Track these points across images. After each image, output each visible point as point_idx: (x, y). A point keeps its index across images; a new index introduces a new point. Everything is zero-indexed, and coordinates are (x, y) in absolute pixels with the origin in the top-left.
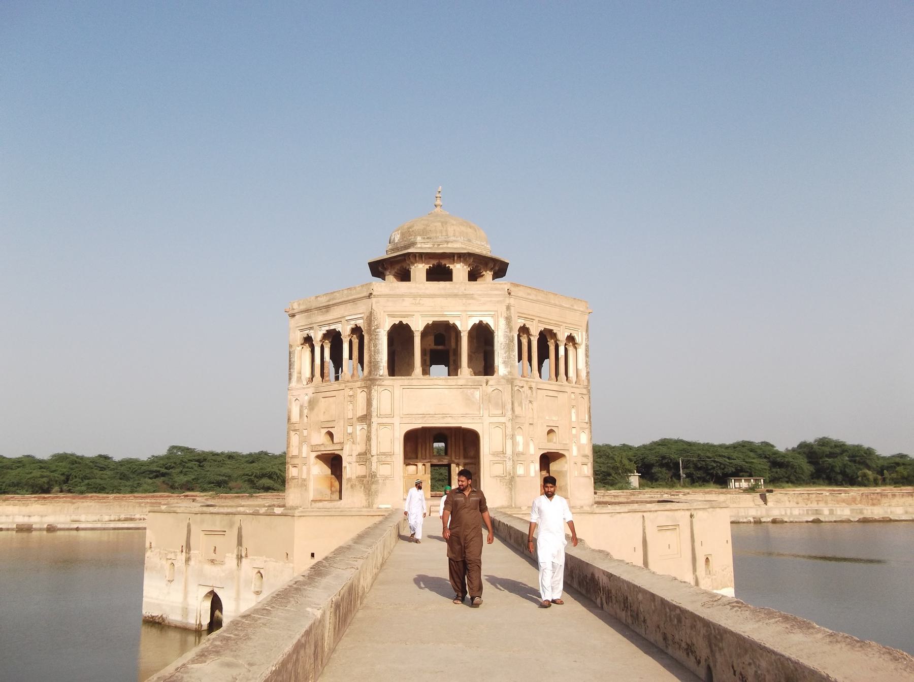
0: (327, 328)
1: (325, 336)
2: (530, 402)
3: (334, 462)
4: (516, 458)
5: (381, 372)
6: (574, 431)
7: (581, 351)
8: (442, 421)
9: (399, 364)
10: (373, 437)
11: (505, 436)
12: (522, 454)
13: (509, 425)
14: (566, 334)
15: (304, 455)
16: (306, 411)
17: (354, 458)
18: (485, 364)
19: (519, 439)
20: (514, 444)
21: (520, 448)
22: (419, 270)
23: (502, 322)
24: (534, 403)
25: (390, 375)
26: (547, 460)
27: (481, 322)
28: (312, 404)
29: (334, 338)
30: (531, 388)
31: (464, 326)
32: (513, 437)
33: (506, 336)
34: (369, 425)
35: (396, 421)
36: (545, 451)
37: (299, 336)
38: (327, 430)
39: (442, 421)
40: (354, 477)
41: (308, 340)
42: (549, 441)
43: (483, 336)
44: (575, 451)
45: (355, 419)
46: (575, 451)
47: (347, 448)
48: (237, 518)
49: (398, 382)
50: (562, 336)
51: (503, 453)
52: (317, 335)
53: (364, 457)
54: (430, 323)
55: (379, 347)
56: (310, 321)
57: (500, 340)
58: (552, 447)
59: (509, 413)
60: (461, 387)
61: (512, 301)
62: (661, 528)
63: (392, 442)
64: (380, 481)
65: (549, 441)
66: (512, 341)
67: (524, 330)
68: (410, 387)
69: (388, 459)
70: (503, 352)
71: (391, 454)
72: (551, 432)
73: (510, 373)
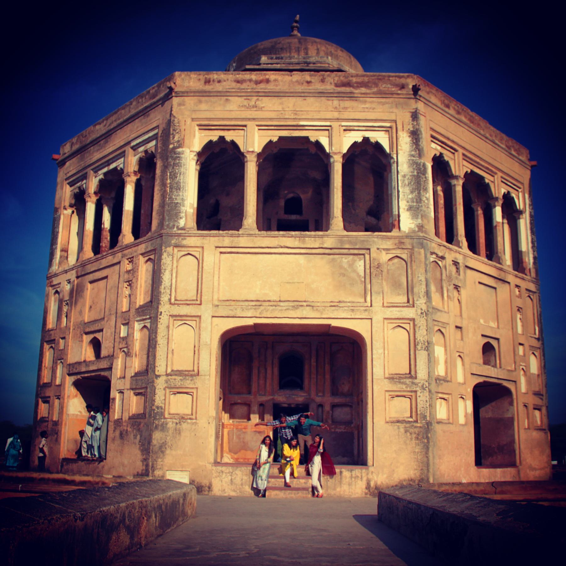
0: (105, 170)
2: (457, 287)
4: (433, 387)
5: (182, 223)
6: (521, 350)
8: (292, 314)
9: (216, 214)
10: (161, 340)
11: (413, 345)
12: (445, 380)
13: (421, 322)
14: (503, 191)
15: (58, 382)
16: (65, 309)
17: (127, 384)
18: (372, 212)
19: (439, 351)
21: (441, 371)
23: (405, 140)
24: (463, 291)
25: (199, 228)
27: (366, 140)
30: (456, 263)
32: (428, 347)
34: (155, 319)
35: (206, 311)
36: (481, 380)
38: (91, 336)
39: (292, 314)
40: (126, 417)
42: (486, 362)
45: (133, 311)
47: (119, 364)
50: (499, 190)
51: (411, 375)
54: (275, 139)
55: (181, 178)
56: (83, 164)
58: (492, 373)
59: (421, 302)
60: (329, 252)
63: (196, 351)
64: (171, 425)
65: (486, 362)
66: (424, 172)
68: (233, 250)
69: (188, 383)
70: (407, 190)
71: (193, 374)
73: (421, 228)
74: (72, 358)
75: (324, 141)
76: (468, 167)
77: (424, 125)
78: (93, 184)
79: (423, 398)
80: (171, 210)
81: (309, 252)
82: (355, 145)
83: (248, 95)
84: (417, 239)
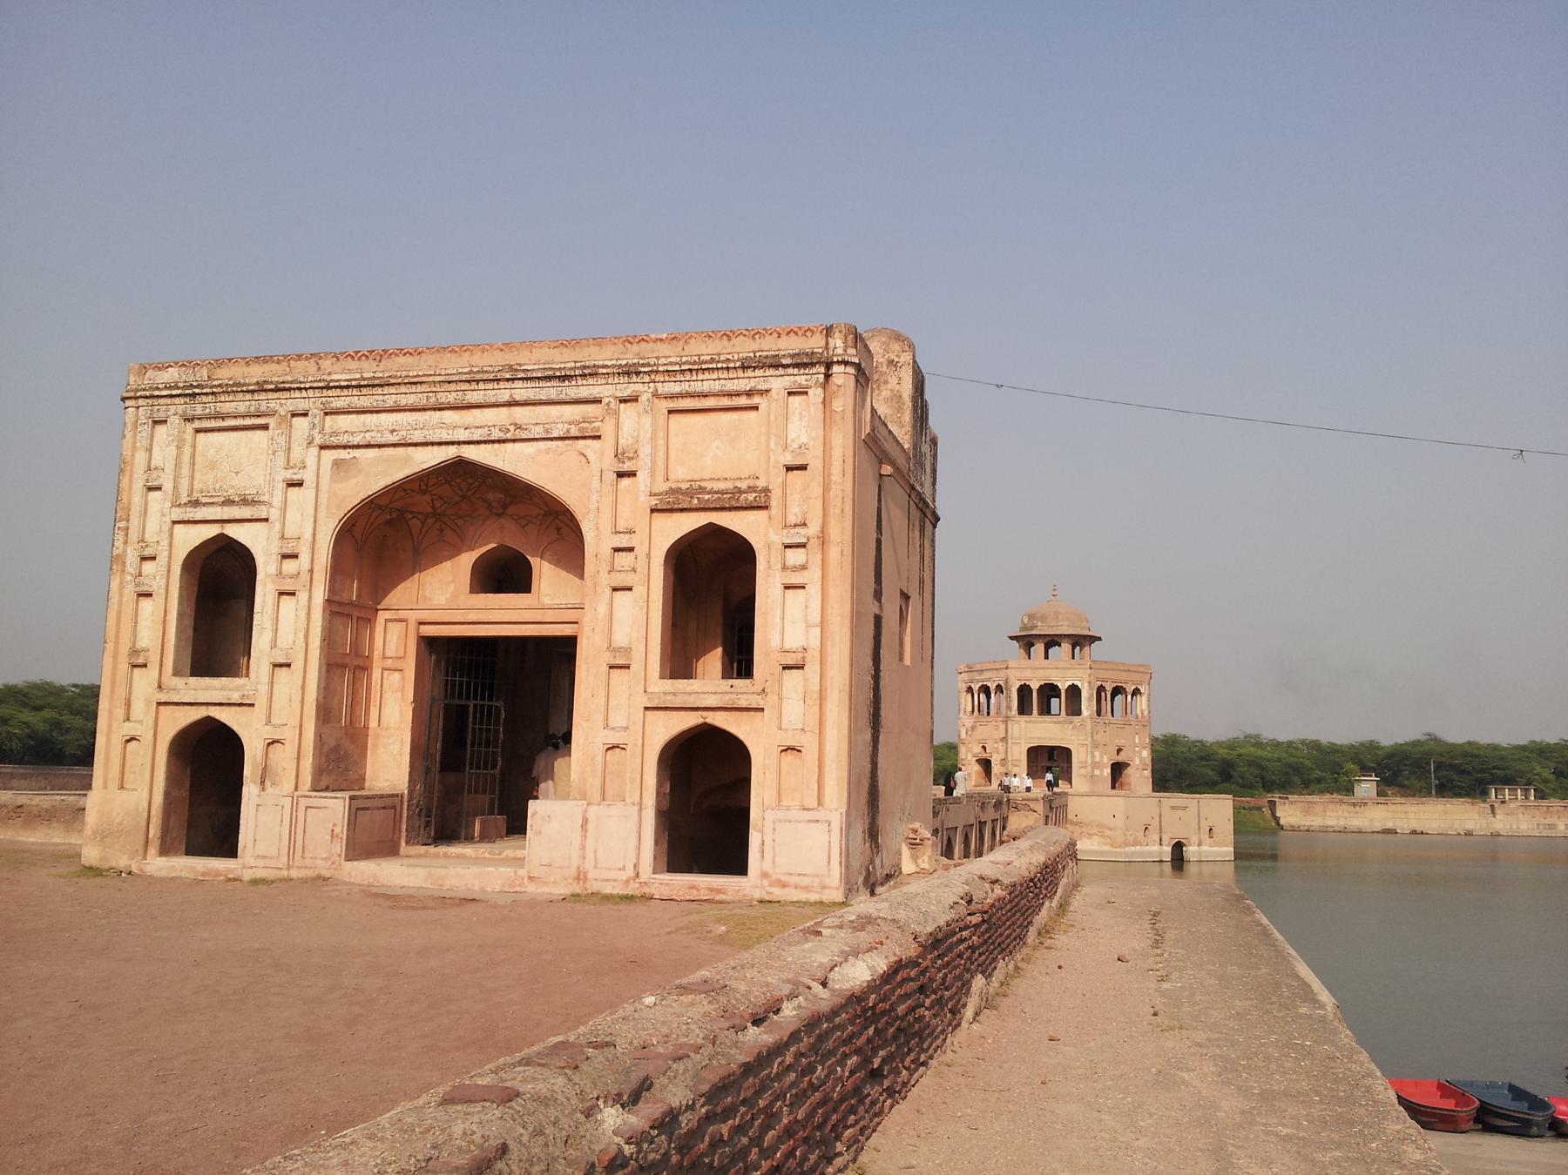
3: (986, 765)
7: (1144, 698)
9: (1024, 708)
18: (1074, 709)
19: (1097, 754)
22: (1039, 648)
26: (1118, 769)
28: (973, 728)
37: (964, 687)
41: (970, 690)
43: (1074, 692)
44: (1137, 761)
46: (1137, 761)
50: (1130, 689)
52: (976, 687)
57: (1084, 695)
58: (1122, 758)
62: (1173, 808)
67: (1101, 689)
72: (1119, 751)
80: (1009, 708)
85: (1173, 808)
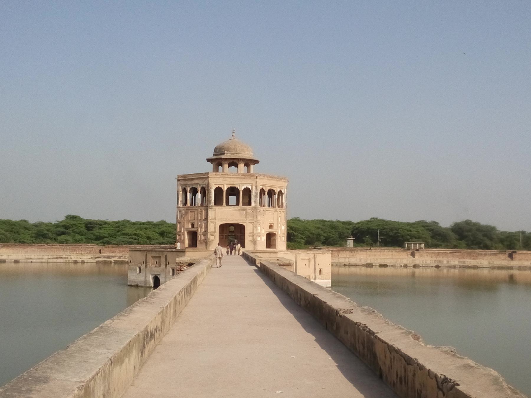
1: (191, 189)
7: (284, 196)
19: (259, 228)
20: (257, 230)
21: (259, 231)
23: (254, 188)
29: (194, 191)
31: (241, 188)
32: (256, 227)
33: (256, 193)
34: (207, 222)
35: (217, 221)
43: (247, 192)
44: (279, 233)
48: (165, 253)
49: (217, 208)
50: (277, 191)
51: (253, 232)
53: (206, 233)
58: (271, 231)
60: (239, 210)
61: (258, 180)
67: (262, 191)
72: (271, 227)
74: (186, 227)
75: (239, 188)
76: (269, 188)
77: (258, 184)
78: (188, 189)
79: (255, 236)
80: (209, 201)
81: (235, 210)
82: (245, 189)
83: (224, 178)
84: (255, 208)
85: (303, 259)
